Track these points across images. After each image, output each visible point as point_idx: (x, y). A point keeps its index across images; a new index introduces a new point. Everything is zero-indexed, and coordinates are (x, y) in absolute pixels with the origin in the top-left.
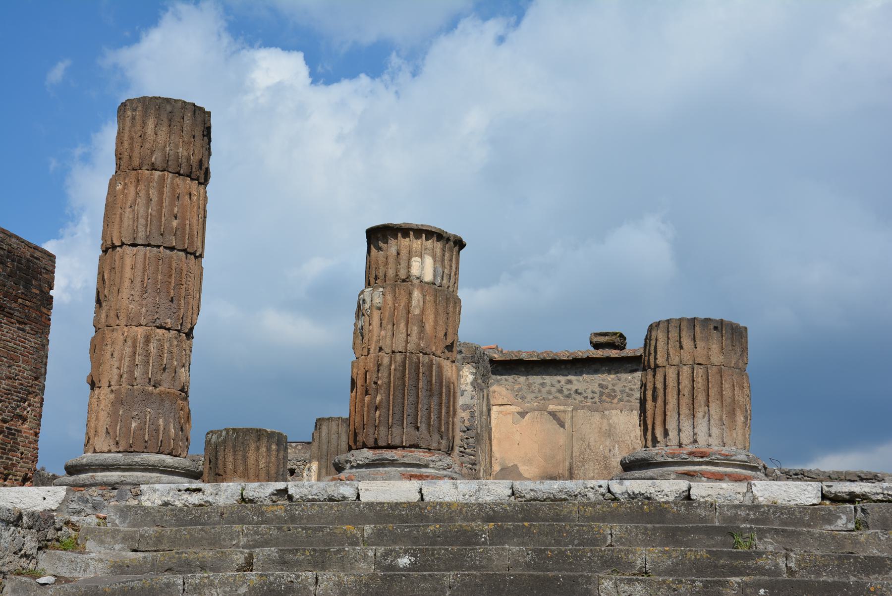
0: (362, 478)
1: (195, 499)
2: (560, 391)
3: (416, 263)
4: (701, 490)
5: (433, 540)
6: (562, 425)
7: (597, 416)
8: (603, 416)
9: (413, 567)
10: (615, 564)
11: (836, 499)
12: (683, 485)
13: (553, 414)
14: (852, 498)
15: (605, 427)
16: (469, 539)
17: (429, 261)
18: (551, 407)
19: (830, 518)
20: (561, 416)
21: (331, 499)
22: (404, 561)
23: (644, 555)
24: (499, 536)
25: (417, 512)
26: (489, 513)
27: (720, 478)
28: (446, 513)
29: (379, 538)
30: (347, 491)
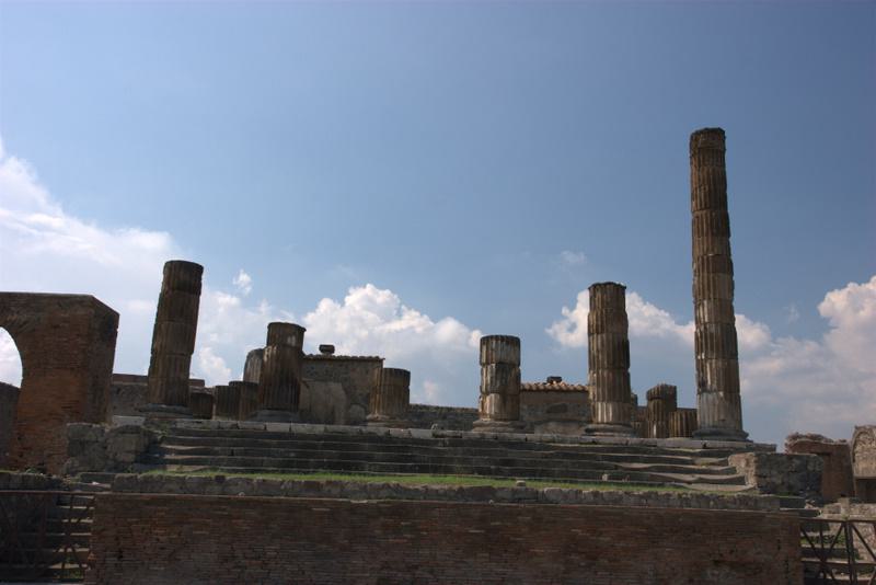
1: (200, 426)
4: (394, 431)
10: (369, 458)
11: (437, 436)
12: (387, 429)
16: (315, 447)
17: (294, 338)
19: (436, 443)
22: (292, 455)
24: (325, 446)
25: (290, 435)
26: (318, 437)
28: (303, 437)
29: (279, 445)
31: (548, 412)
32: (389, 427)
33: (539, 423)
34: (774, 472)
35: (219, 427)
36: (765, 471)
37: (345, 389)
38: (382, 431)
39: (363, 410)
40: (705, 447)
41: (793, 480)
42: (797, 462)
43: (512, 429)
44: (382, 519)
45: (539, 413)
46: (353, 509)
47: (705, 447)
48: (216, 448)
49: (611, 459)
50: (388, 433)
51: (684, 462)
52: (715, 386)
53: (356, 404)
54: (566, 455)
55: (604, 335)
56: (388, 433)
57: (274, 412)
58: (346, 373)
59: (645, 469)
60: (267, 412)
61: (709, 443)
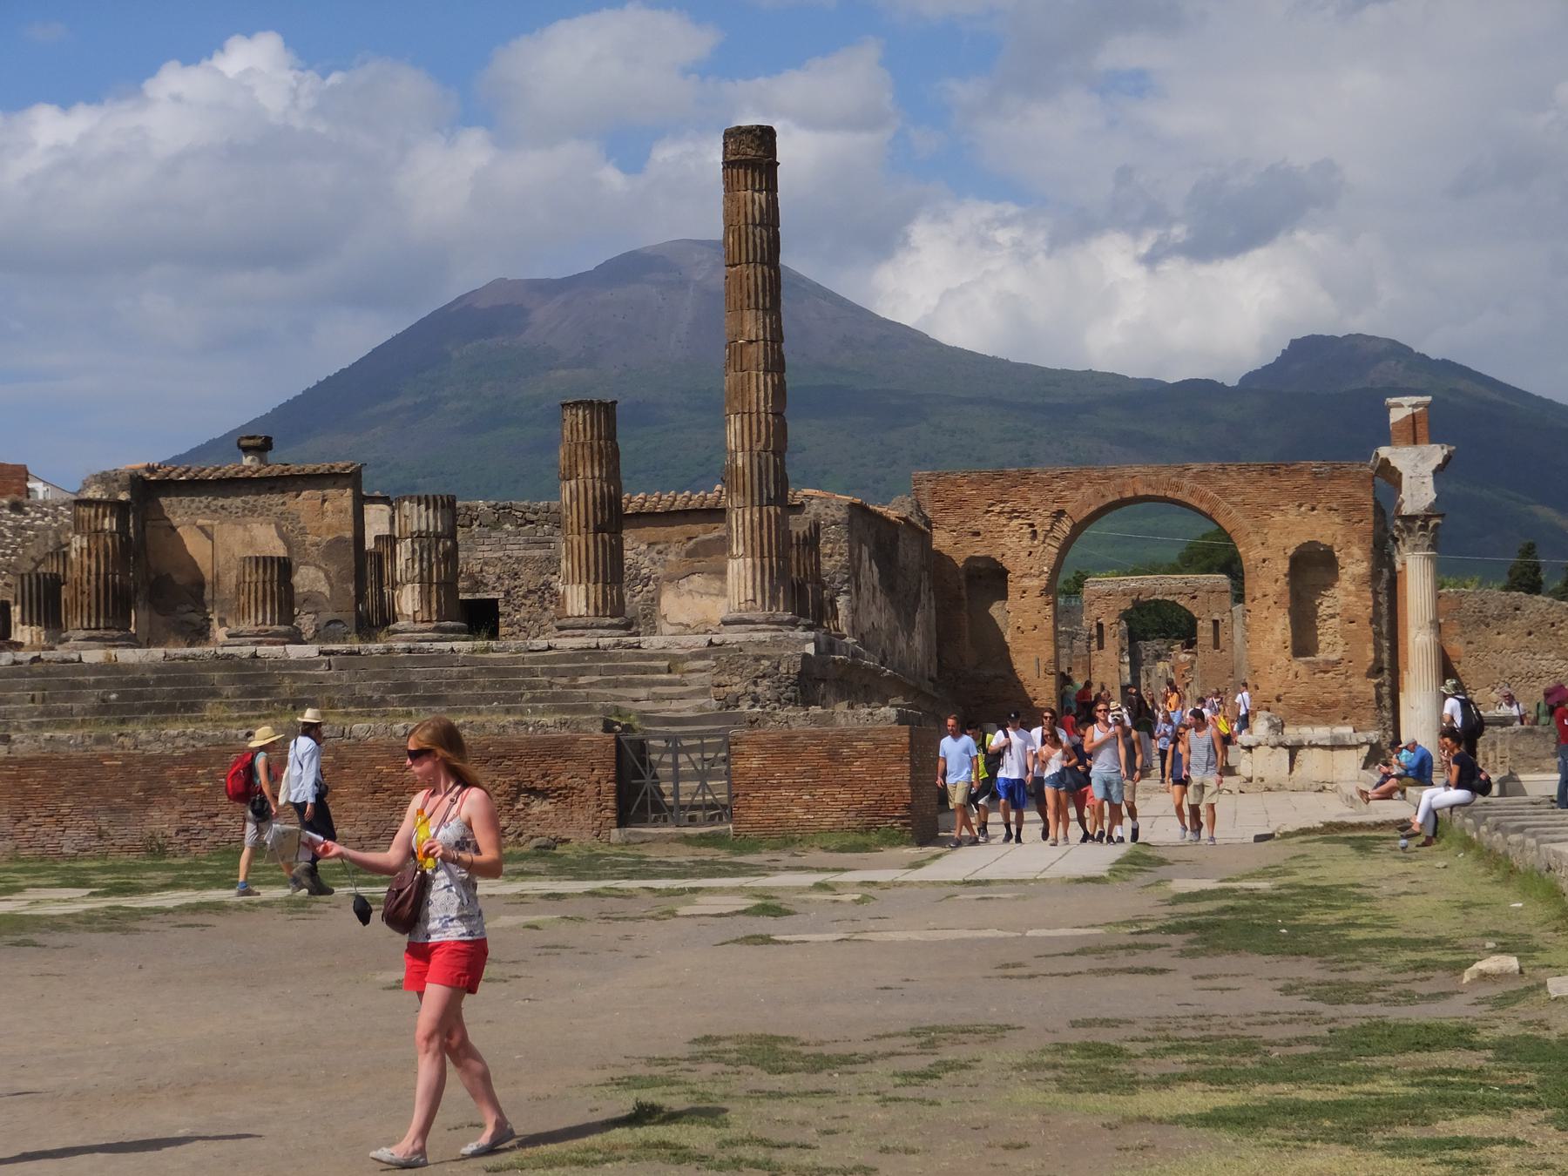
0: (82, 649)
2: (207, 507)
3: (107, 521)
4: (262, 650)
5: (127, 684)
6: (210, 537)
7: (240, 531)
8: (246, 529)
9: (118, 699)
10: (214, 694)
12: (253, 649)
13: (201, 528)
14: (332, 653)
15: (247, 538)
16: (143, 682)
18: (200, 522)
20: (209, 530)
21: (65, 661)
22: (113, 696)
23: (229, 690)
24: (159, 682)
27: (275, 644)
28: (129, 668)
30: (75, 656)
31: (689, 554)
32: (259, 643)
33: (671, 579)
34: (737, 679)
35: (15, 663)
36: (724, 679)
37: (282, 536)
38: (246, 651)
39: (322, 575)
40: (711, 643)
41: (762, 688)
42: (766, 663)
43: (435, 635)
44: (177, 768)
45: (671, 557)
46: (148, 760)
47: (711, 643)
48: (11, 694)
49: (552, 672)
50: (254, 656)
51: (658, 671)
52: (741, 551)
53: (306, 564)
54: (490, 671)
55: (573, 482)
56: (254, 656)
57: (95, 633)
58: (284, 504)
59: (591, 684)
60: (83, 634)
61: (716, 639)
